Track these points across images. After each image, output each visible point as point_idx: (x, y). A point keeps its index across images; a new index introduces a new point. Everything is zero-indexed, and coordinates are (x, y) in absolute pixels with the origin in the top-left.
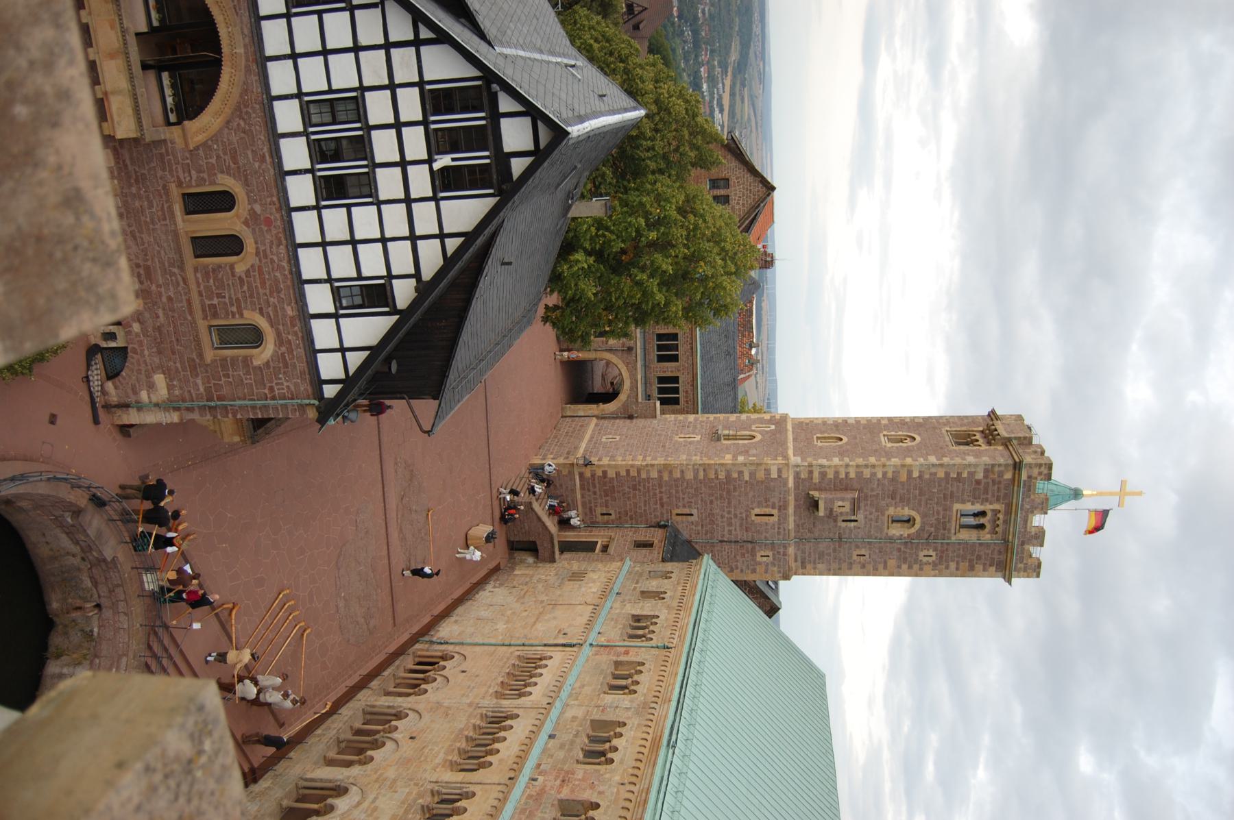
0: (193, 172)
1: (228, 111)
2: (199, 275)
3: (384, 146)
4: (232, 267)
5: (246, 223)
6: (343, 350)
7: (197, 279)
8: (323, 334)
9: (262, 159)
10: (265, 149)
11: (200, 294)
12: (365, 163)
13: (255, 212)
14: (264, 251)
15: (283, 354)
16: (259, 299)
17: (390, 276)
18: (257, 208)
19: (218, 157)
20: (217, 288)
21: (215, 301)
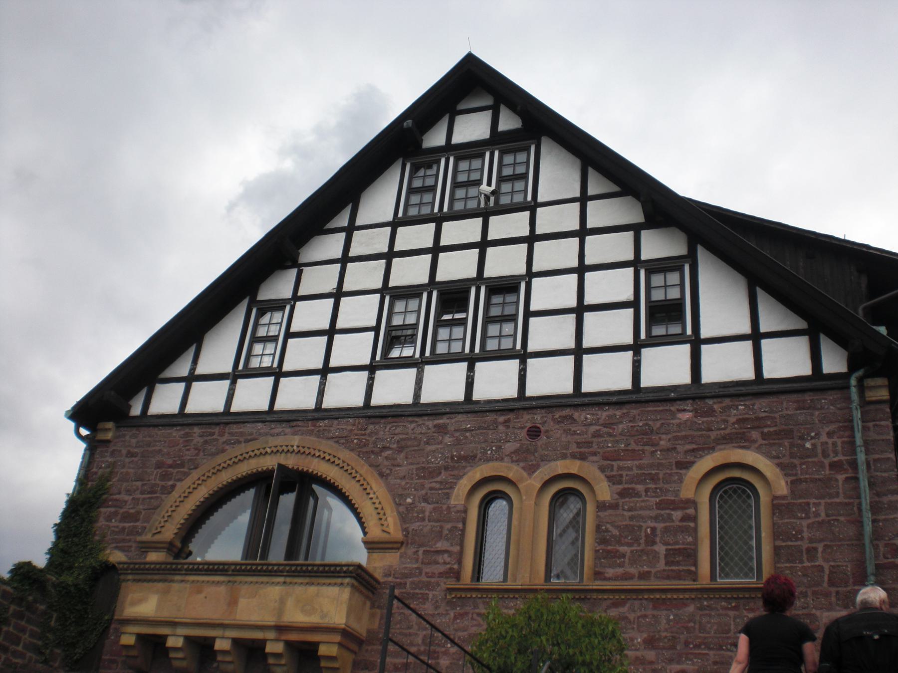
0: (440, 545)
1: (364, 469)
2: (610, 572)
3: (456, 267)
4: (601, 506)
5: (531, 469)
6: (756, 337)
7: (616, 578)
8: (726, 365)
9: (441, 429)
10: (430, 424)
11: (644, 576)
12: (473, 291)
13: (516, 452)
14: (578, 444)
15: (764, 436)
16: (659, 466)
17: (636, 263)
18: (510, 447)
19: (425, 500)
20: (637, 540)
21: (661, 549)
